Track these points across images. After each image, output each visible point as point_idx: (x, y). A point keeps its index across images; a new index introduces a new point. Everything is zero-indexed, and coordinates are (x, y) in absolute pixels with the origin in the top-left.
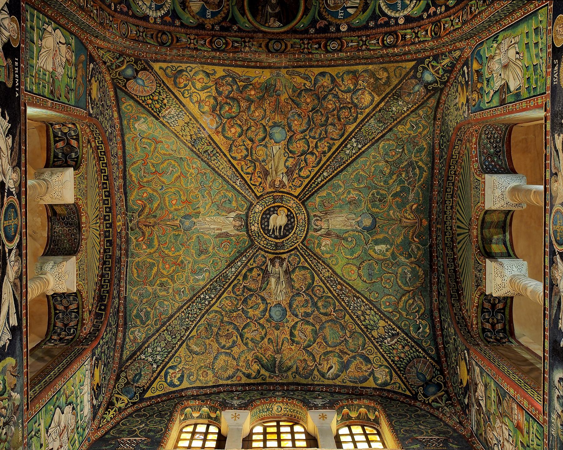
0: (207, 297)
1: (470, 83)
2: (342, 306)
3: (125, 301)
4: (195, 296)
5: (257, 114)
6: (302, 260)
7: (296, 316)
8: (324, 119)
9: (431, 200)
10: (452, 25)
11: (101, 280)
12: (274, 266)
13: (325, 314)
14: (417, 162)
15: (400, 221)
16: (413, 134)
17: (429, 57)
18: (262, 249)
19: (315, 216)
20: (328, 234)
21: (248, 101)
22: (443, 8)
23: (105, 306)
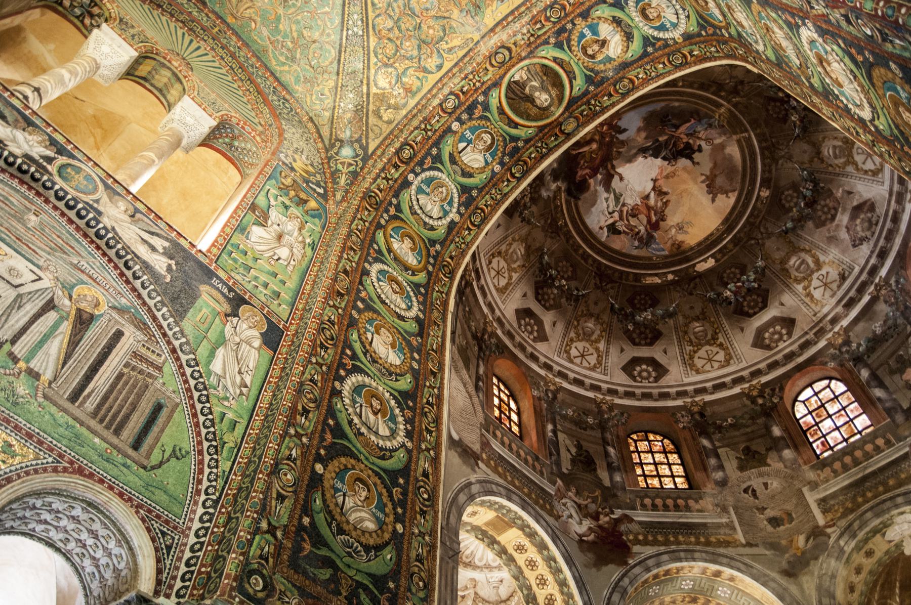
1: (305, 185)
8: (403, 25)
10: (361, 219)
14: (290, 66)
16: (317, 88)
17: (362, 169)
22: (383, 222)
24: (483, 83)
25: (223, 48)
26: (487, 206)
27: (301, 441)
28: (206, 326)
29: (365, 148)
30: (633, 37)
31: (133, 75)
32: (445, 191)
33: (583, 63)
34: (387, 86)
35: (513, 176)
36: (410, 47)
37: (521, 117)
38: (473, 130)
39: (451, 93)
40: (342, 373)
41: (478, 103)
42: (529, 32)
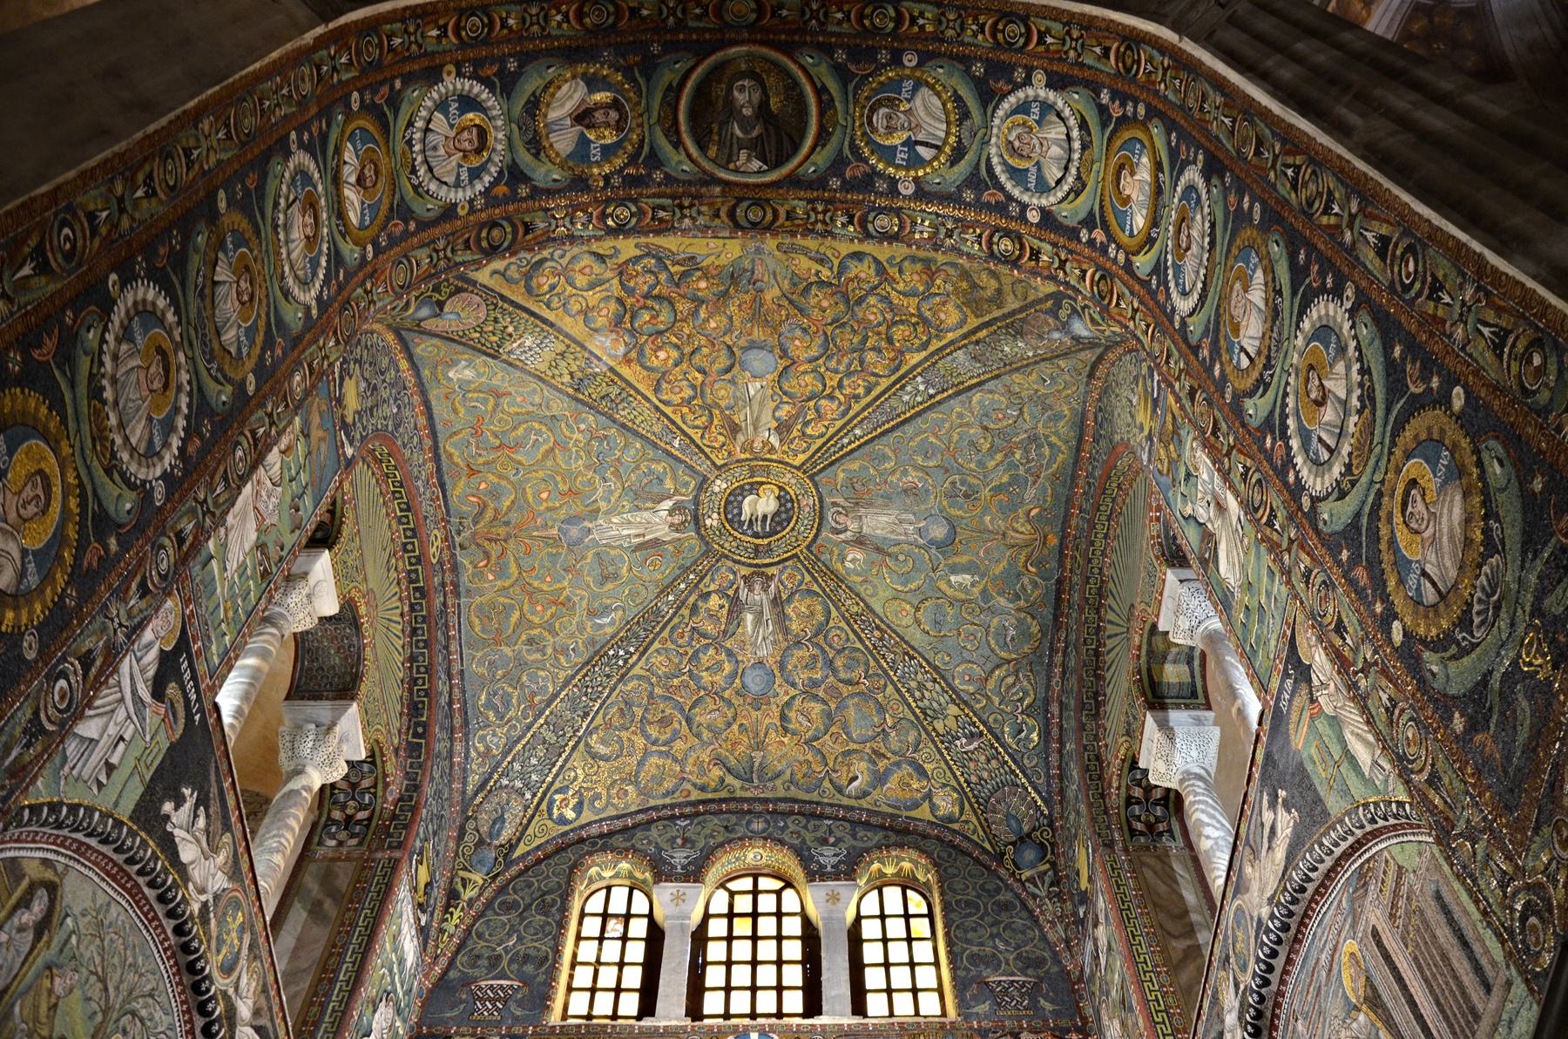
0: (621, 653)
2: (881, 667)
3: (462, 679)
4: (598, 654)
5: (713, 324)
6: (808, 578)
7: (793, 685)
8: (855, 340)
9: (1069, 502)
10: (1133, 318)
11: (411, 668)
12: (751, 590)
13: (849, 682)
14: (1047, 437)
15: (1004, 535)
18: (727, 557)
19: (835, 504)
20: (860, 541)
21: (693, 301)
22: (1121, 257)
23: (424, 725)
24: (810, 201)
25: (1092, 543)
26: (982, 27)
27: (1371, 665)
28: (1328, 758)
29: (1057, 298)
30: (528, 101)
31: (1193, 685)
32: (1014, 134)
33: (639, 103)
34: (950, 307)
35: (899, 20)
36: (873, 311)
37: (802, 95)
38: (888, 154)
39: (868, 236)
40: (1291, 478)
41: (844, 182)
42: (683, 216)
